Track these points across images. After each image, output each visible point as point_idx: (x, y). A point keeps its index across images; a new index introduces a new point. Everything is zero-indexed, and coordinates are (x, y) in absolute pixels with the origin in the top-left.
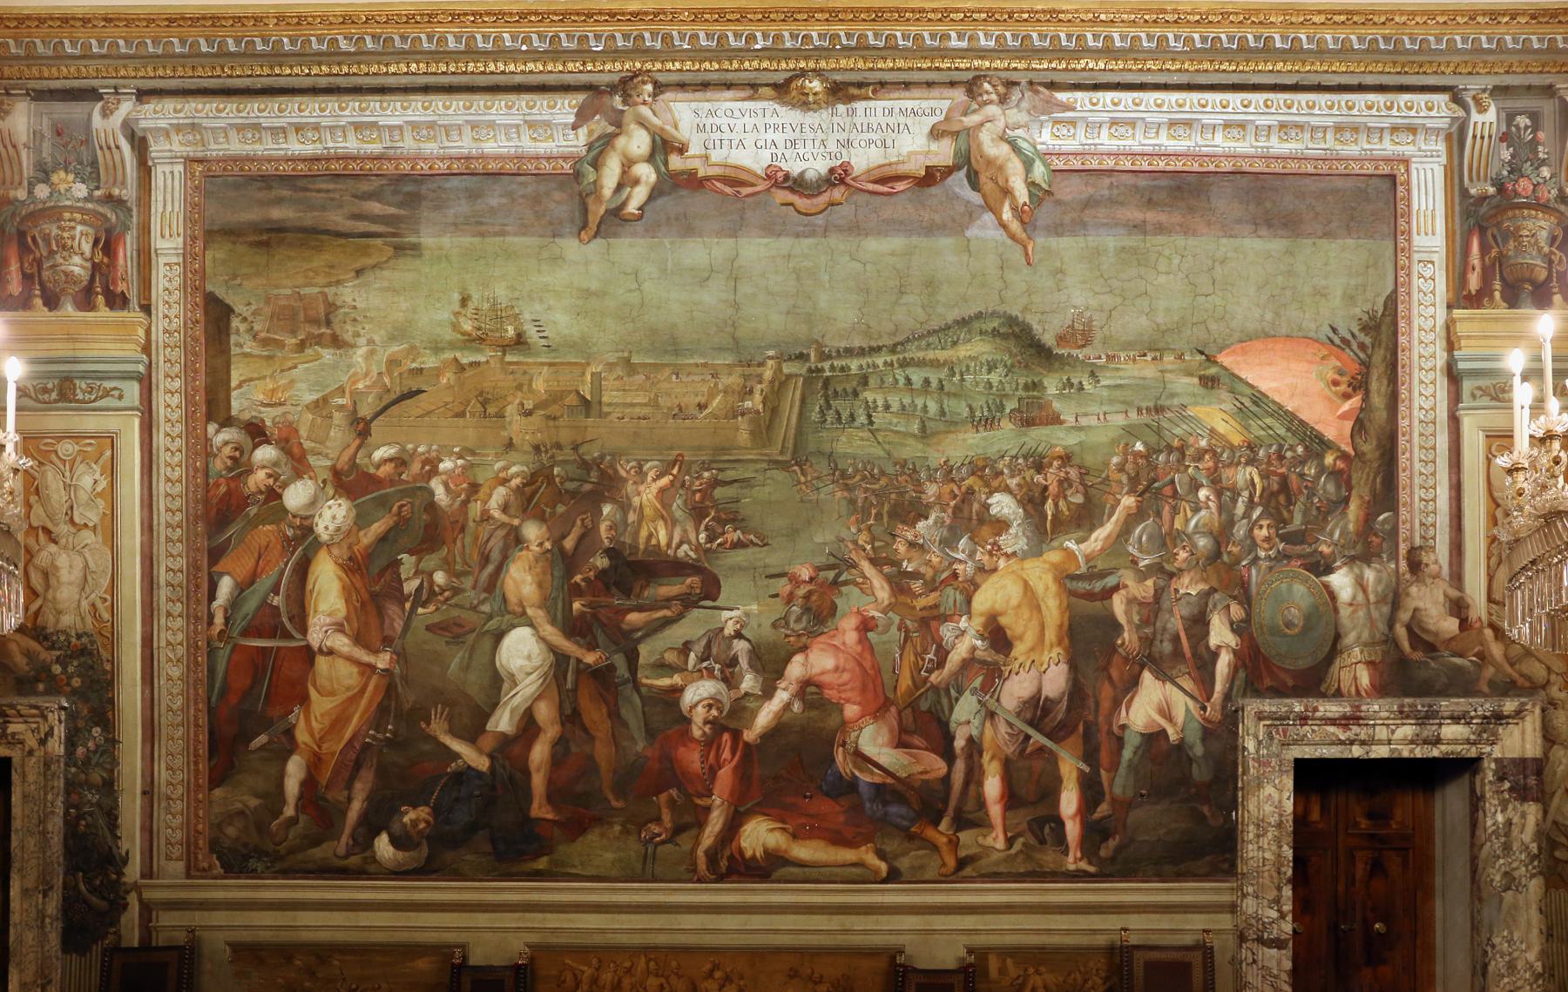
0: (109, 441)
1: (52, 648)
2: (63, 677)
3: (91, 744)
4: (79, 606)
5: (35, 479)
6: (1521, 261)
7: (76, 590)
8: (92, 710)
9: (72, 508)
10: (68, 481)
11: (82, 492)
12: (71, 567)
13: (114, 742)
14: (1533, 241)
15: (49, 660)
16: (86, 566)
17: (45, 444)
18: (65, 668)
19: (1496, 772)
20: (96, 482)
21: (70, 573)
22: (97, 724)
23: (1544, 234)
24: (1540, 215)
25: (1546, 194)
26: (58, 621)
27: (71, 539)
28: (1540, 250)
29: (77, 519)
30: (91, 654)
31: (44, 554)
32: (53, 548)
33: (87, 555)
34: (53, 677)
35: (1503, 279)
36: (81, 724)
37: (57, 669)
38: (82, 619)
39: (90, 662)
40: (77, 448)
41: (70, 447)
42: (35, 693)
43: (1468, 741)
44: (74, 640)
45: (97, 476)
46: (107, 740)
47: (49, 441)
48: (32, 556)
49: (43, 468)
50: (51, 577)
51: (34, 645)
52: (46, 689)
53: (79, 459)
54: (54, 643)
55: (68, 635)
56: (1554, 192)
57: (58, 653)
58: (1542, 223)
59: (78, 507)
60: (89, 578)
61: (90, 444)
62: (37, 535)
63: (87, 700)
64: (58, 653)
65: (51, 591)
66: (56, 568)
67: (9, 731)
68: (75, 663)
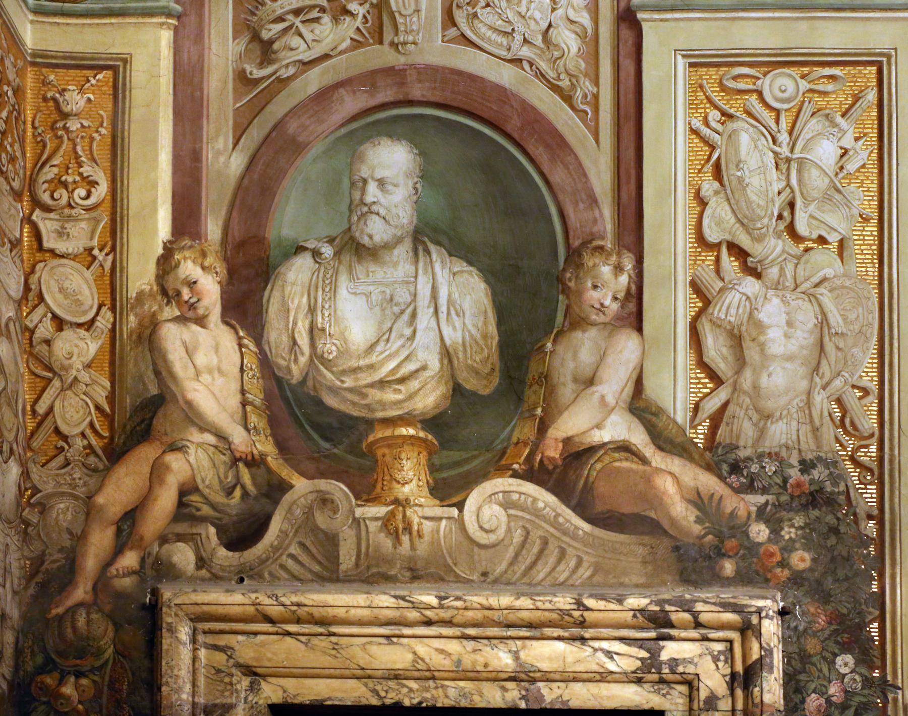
0: (874, 69)
1: (750, 487)
2: (774, 548)
3: (834, 689)
4: (809, 403)
5: (713, 148)
7: (802, 371)
8: (837, 618)
9: (792, 205)
10: (784, 151)
11: (815, 173)
12: (790, 324)
13: (885, 687)
15: (742, 513)
16: (823, 321)
17: (735, 78)
18: (776, 531)
20: (845, 152)
21: (787, 336)
22: (846, 648)
26: (762, 433)
27: (789, 272)
29: (802, 228)
30: (831, 502)
31: (733, 298)
32: (751, 285)
33: (827, 301)
34: (752, 548)
36: (812, 645)
37: (760, 532)
38: (815, 430)
39: (830, 519)
40: (804, 85)
41: (790, 85)
42: (716, 579)
44: (794, 474)
45: (848, 141)
46: (868, 682)
47: (746, 70)
48: (707, 302)
49: (732, 125)
50: (747, 344)
51: (708, 482)
52: (738, 572)
53: (808, 109)
54: (752, 479)
55: (782, 463)
57: (761, 499)
59: (807, 201)
60: (829, 347)
61: (832, 78)
62: (718, 261)
63: (825, 598)
64: (761, 499)
65: (748, 374)
66: (760, 327)
67: (664, 656)
68: (799, 521)
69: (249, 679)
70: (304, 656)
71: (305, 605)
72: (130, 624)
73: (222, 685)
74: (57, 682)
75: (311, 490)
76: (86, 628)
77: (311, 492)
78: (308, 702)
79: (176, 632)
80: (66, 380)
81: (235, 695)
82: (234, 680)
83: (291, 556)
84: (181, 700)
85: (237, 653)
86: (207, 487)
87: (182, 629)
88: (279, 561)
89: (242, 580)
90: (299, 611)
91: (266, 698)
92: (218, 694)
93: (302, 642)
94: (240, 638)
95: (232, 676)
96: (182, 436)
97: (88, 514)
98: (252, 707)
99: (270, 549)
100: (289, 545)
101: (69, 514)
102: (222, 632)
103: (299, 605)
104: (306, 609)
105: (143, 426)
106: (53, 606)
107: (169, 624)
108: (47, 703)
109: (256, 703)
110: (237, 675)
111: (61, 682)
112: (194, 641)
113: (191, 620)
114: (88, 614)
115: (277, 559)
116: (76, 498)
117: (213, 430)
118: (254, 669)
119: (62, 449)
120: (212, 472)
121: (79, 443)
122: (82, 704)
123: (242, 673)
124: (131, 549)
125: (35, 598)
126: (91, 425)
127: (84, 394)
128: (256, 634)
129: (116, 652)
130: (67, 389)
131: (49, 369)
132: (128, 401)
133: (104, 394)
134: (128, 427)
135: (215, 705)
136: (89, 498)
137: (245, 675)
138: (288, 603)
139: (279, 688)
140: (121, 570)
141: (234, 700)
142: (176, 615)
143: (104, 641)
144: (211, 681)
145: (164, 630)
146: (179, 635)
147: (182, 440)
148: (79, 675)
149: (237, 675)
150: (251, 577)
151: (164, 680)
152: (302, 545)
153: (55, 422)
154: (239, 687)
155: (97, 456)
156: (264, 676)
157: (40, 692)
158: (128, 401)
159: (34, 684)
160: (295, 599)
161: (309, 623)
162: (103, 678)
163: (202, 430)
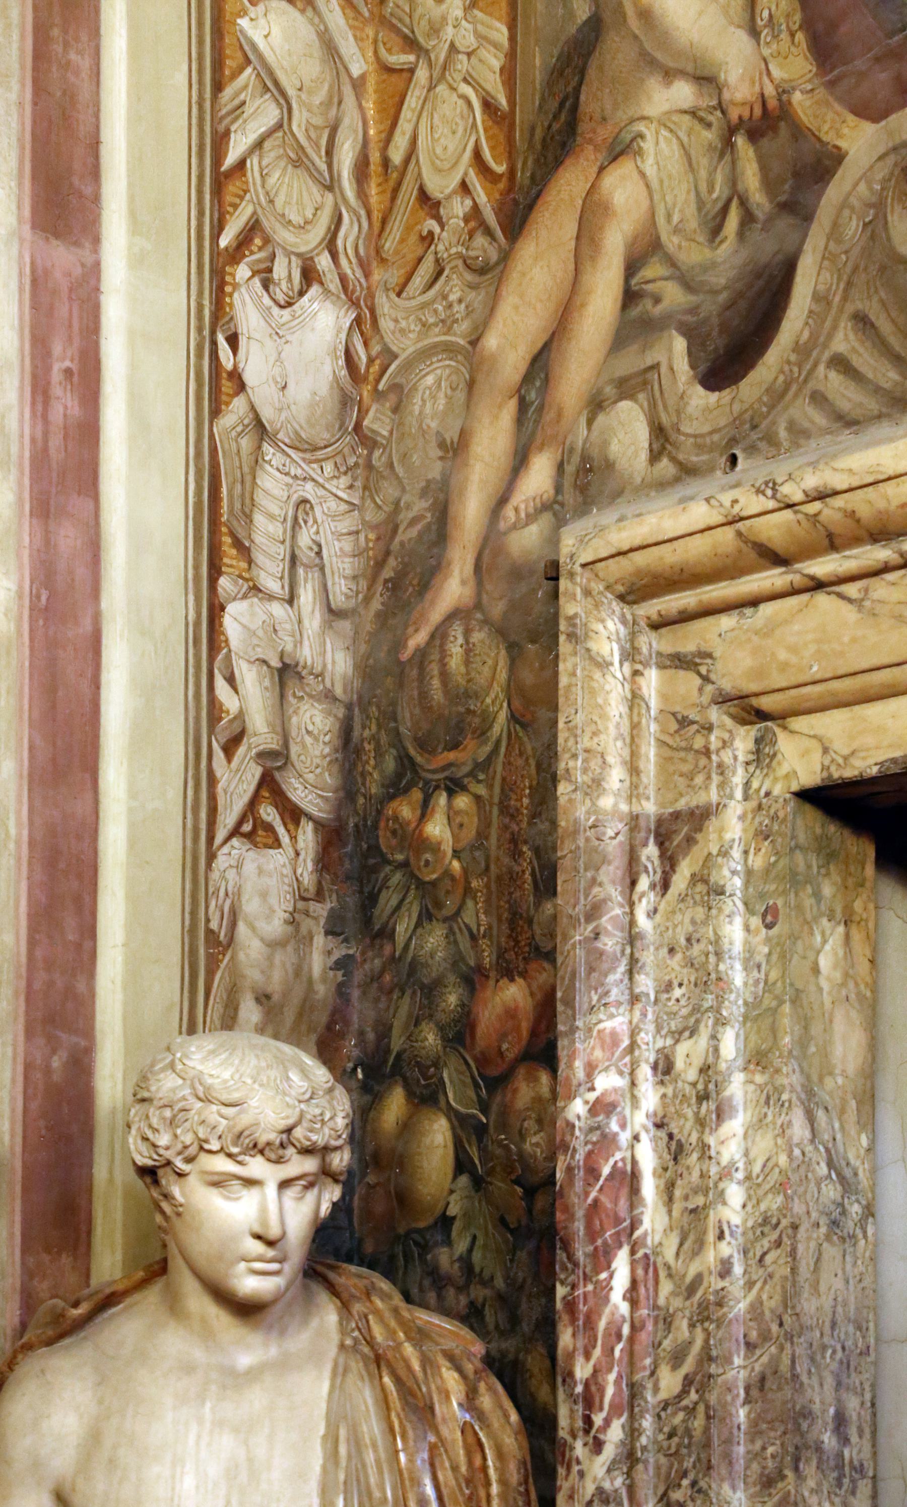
69: (753, 731)
70: (854, 640)
71: (836, 493)
72: (533, 642)
73: (690, 757)
74: (419, 812)
75: (882, 150)
76: (463, 670)
77: (881, 158)
78: (875, 770)
79: (587, 636)
80: (437, 59)
81: (716, 779)
82: (714, 740)
83: (841, 364)
84: (595, 810)
85: (719, 665)
86: (676, 231)
87: (599, 627)
88: (811, 385)
89: (733, 460)
90: (827, 512)
91: (787, 776)
92: (681, 782)
93: (850, 600)
94: (726, 622)
95: (710, 728)
96: (632, 112)
97: (471, 385)
98: (760, 807)
99: (793, 358)
100: (830, 336)
101: (441, 395)
102: (685, 617)
103: (823, 495)
104: (838, 502)
105: (563, 117)
106: (410, 630)
107: (571, 619)
108: (405, 864)
109: (767, 794)
110: (722, 726)
111: (425, 810)
112: (630, 654)
113: (621, 598)
114: (467, 633)
115: (806, 381)
116: (449, 349)
117: (690, 68)
118: (754, 702)
119: (429, 239)
120: (684, 186)
121: (458, 208)
122: (459, 859)
123: (733, 717)
124: (541, 449)
125: (383, 618)
126: (477, 155)
127: (465, 80)
128: (754, 602)
129: (513, 718)
130: (439, 81)
131: (411, 44)
132: (538, 62)
133: (496, 63)
134: (539, 133)
135: (676, 815)
136: (474, 343)
137: (743, 722)
138: (798, 497)
139: (814, 744)
140: (522, 506)
141: (714, 796)
142: (587, 593)
143: (492, 695)
144: (669, 753)
145: (562, 638)
146: (592, 645)
147: (632, 121)
148: (454, 787)
149: (722, 726)
150: (751, 450)
151: (562, 765)
152: (862, 321)
153: (420, 174)
154: (726, 757)
155: (488, 232)
156: (781, 717)
157: (394, 842)
158: (538, 62)
159: (382, 824)
160: (811, 481)
161: (856, 541)
162: (490, 787)
163: (669, 75)
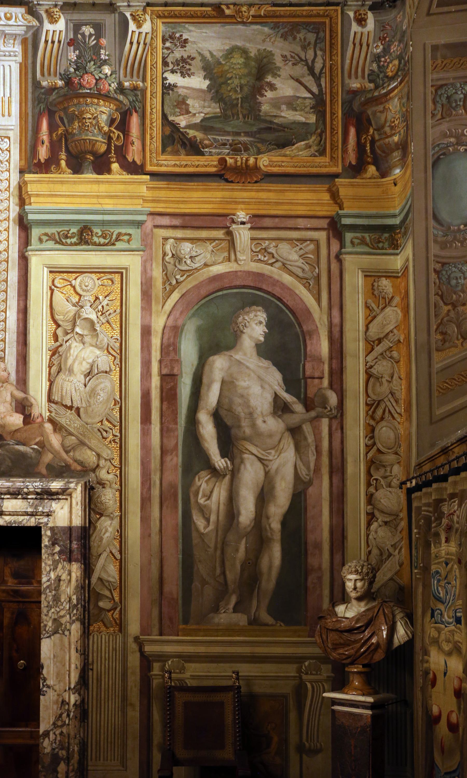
6: (84, 137)
14: (94, 122)
19: (50, 538)
23: (104, 117)
24: (102, 102)
25: (107, 86)
28: (100, 129)
35: (67, 151)
43: (26, 514)
56: (114, 86)
58: (103, 109)
